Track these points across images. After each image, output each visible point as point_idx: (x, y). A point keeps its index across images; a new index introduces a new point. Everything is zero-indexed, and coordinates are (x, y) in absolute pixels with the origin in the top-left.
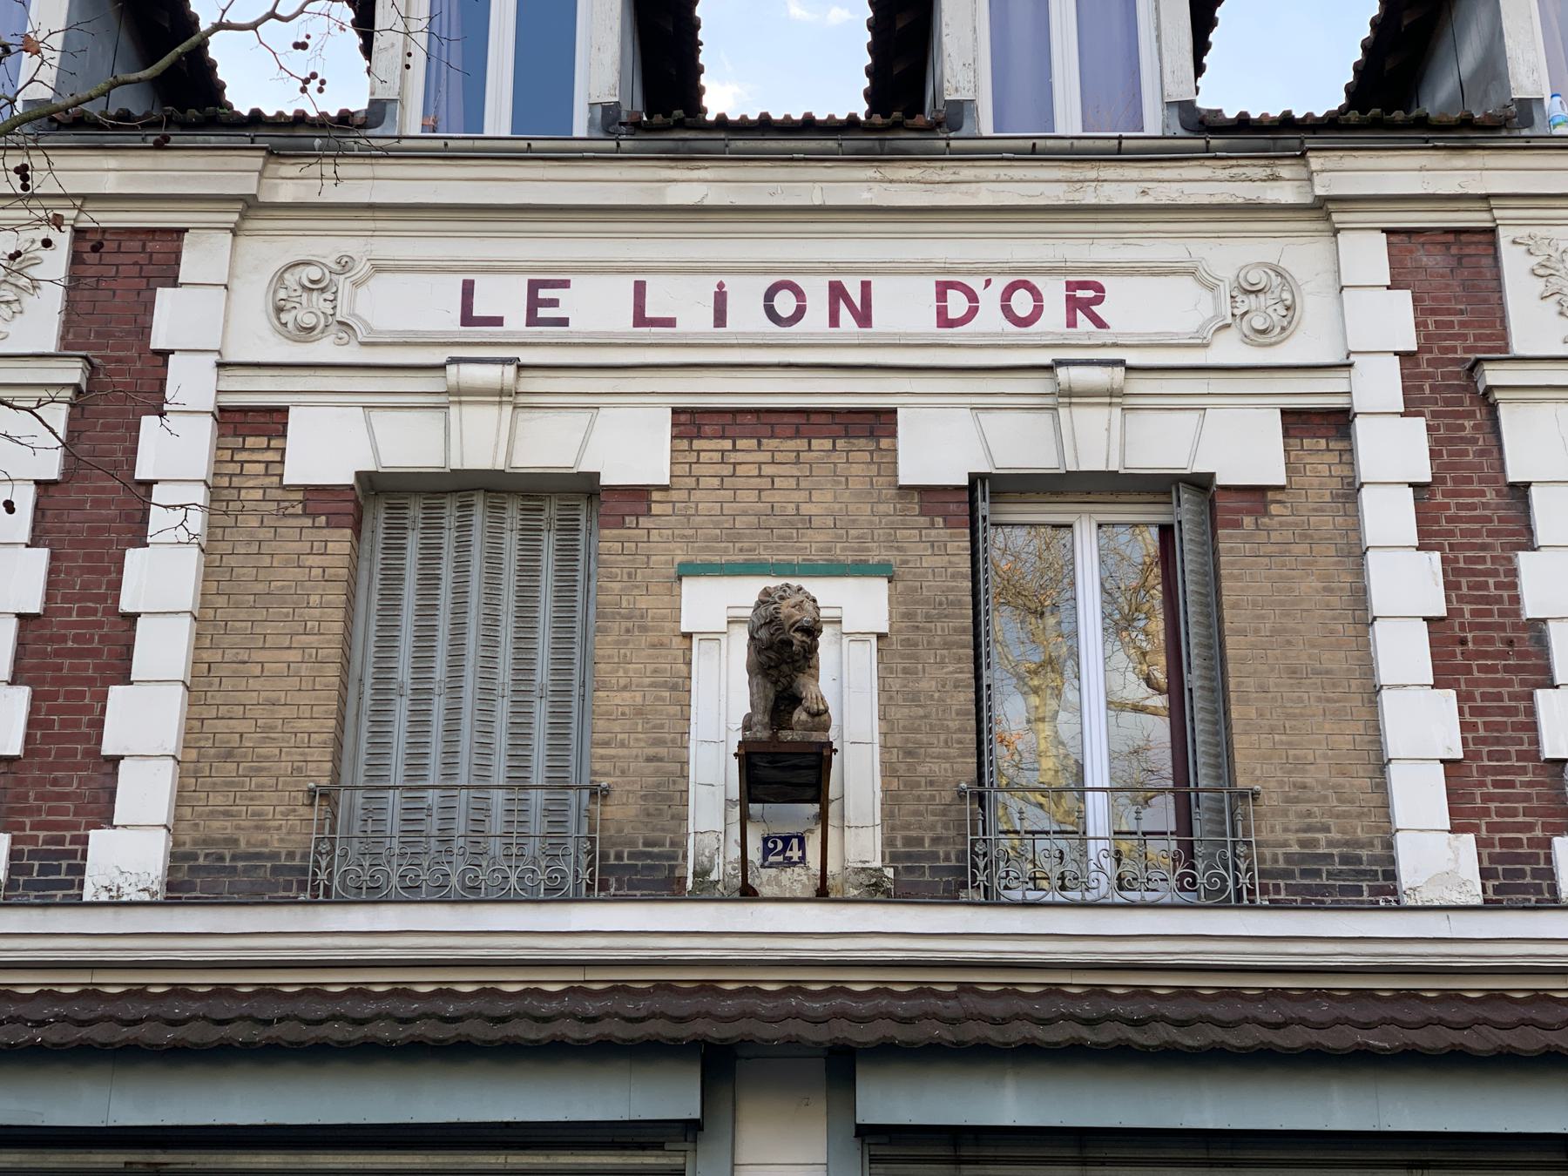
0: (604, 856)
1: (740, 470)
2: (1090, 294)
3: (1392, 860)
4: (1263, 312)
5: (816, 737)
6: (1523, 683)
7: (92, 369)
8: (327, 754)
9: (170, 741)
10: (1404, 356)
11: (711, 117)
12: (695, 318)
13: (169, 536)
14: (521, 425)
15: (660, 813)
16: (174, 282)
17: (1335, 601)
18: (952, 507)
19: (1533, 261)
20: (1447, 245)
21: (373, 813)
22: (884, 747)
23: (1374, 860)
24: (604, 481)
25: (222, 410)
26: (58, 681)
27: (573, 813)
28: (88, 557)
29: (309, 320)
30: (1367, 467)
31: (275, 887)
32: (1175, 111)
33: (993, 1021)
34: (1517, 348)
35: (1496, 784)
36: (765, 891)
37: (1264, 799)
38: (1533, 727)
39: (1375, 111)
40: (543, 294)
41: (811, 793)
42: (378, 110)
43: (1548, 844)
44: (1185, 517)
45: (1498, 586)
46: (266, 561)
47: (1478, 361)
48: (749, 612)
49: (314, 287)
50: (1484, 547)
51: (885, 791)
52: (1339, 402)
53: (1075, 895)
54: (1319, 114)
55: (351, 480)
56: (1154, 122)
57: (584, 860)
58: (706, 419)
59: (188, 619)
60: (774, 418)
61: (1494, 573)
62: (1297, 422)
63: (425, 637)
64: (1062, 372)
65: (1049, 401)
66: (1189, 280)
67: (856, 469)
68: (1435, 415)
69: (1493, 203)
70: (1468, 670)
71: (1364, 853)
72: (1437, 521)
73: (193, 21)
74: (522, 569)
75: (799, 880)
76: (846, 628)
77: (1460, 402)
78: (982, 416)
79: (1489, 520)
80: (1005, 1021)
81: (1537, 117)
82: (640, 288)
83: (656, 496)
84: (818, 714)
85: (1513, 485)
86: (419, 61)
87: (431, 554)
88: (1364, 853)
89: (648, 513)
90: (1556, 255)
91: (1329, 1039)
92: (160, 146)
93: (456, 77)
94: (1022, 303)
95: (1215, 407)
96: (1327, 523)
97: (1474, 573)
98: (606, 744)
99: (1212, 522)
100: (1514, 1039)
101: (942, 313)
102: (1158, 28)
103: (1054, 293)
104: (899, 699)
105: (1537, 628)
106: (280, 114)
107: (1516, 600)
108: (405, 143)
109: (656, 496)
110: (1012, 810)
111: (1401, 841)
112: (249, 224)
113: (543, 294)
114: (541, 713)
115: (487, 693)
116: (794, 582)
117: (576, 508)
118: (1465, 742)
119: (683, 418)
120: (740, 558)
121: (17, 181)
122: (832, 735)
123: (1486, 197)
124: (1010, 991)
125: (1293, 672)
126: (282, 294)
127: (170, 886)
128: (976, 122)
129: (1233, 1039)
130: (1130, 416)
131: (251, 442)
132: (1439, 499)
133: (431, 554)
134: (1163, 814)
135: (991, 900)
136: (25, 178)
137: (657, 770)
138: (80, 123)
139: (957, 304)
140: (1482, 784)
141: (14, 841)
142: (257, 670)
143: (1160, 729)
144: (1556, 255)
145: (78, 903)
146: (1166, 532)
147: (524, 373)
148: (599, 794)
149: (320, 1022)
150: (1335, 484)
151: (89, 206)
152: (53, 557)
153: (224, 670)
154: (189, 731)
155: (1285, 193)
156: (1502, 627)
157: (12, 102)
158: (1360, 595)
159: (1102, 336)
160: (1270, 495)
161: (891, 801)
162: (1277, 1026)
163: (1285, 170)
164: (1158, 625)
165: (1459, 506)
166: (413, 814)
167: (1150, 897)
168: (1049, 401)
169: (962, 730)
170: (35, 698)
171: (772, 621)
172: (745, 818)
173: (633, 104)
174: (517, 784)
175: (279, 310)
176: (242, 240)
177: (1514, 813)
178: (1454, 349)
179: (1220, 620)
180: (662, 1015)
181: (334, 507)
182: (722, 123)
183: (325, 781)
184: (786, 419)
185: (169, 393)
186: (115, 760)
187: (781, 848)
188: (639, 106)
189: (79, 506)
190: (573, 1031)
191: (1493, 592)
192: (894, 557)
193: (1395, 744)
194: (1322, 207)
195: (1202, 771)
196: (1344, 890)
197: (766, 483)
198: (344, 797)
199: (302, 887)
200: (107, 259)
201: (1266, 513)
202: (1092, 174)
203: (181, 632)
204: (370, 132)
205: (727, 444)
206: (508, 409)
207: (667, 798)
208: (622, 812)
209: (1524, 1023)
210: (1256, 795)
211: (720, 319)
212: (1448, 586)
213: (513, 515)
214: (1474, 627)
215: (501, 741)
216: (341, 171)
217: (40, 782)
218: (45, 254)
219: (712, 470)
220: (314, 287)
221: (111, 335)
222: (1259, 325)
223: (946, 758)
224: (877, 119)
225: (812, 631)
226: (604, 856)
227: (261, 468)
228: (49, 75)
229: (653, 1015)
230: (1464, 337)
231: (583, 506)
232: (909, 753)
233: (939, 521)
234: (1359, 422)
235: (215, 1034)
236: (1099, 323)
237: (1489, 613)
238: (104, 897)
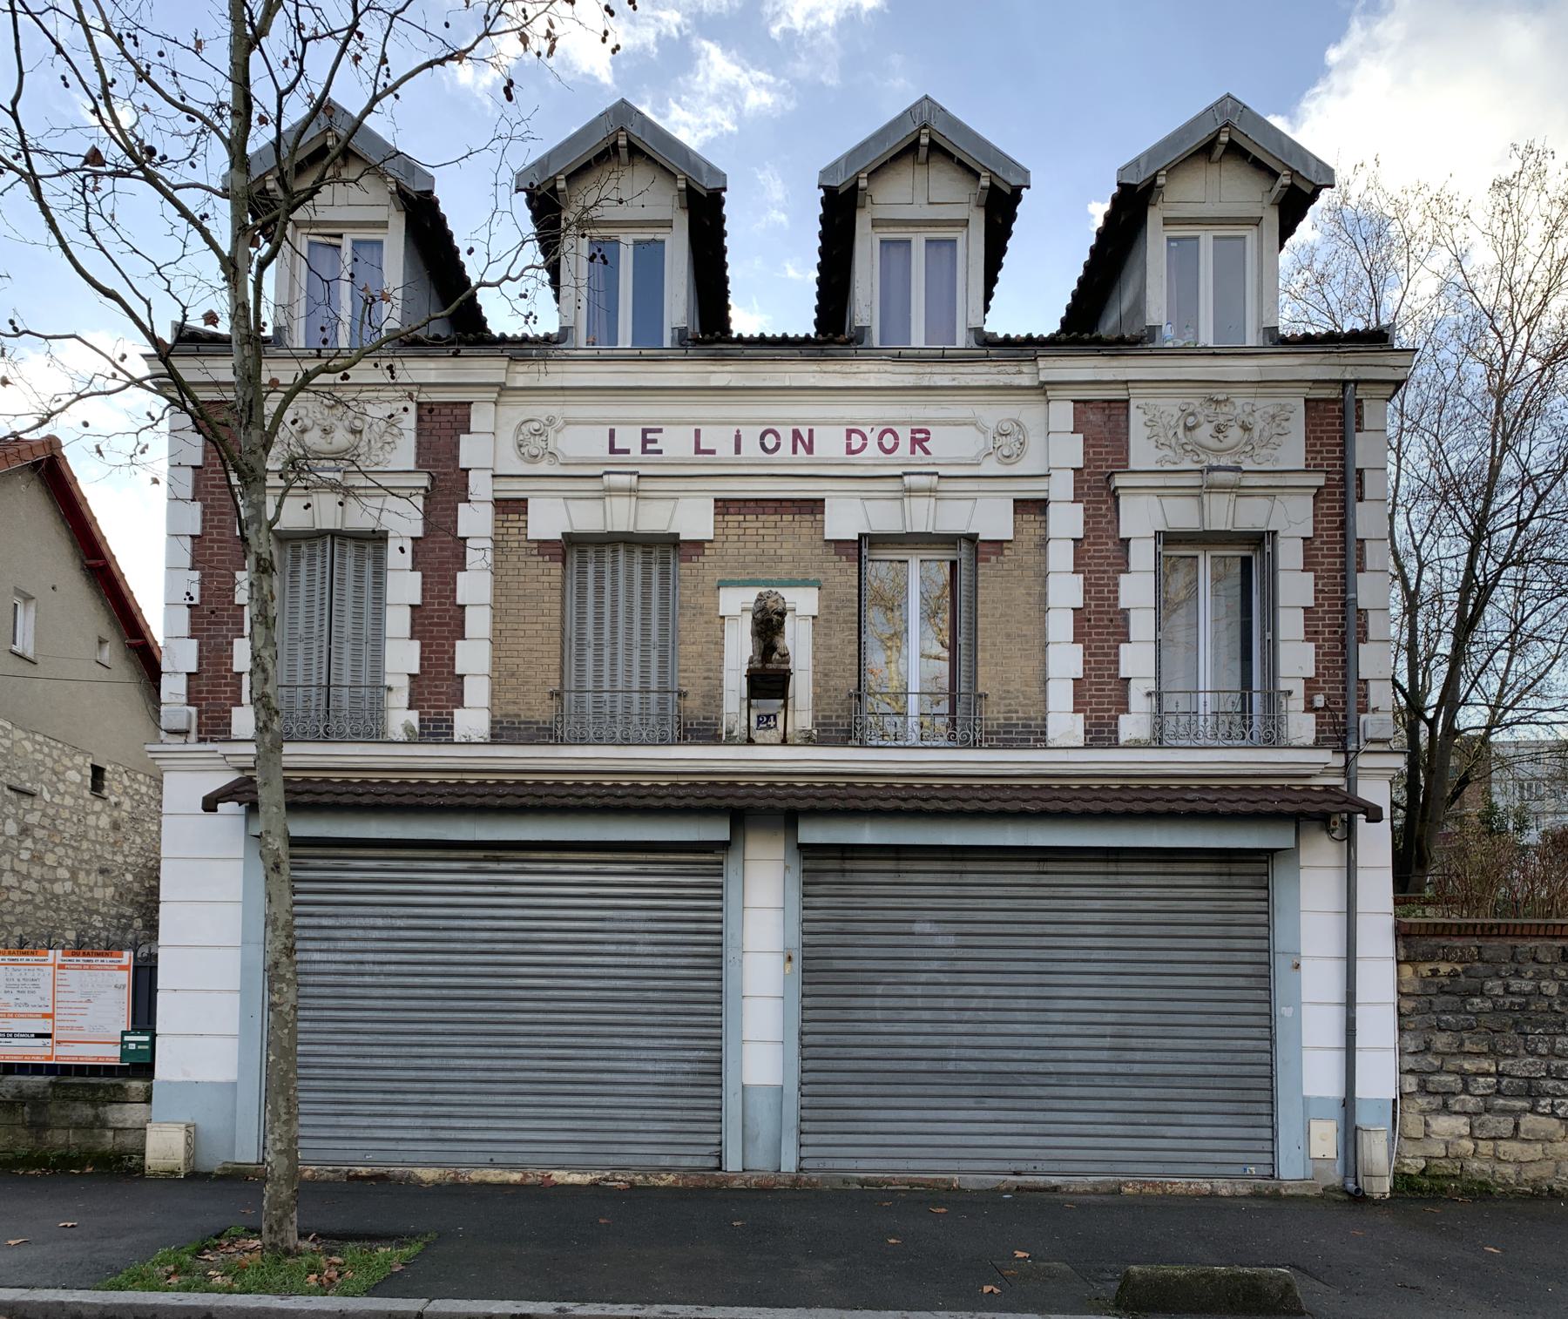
0: (685, 724)
1: (748, 531)
2: (923, 436)
3: (1045, 726)
4: (1008, 448)
5: (783, 666)
6: (1115, 640)
7: (433, 479)
8: (557, 675)
9: (486, 669)
10: (1076, 470)
11: (734, 335)
12: (725, 451)
13: (477, 565)
14: (640, 508)
15: (710, 704)
16: (468, 432)
17: (1031, 600)
18: (851, 551)
19: (1147, 417)
20: (1104, 409)
21: (580, 703)
22: (814, 672)
23: (1037, 726)
24: (682, 538)
25: (496, 500)
26: (432, 638)
27: (670, 704)
28: (440, 576)
29: (535, 452)
30: (1053, 531)
31: (538, 736)
32: (973, 333)
33: (862, 799)
34: (1132, 467)
35: (1096, 690)
36: (758, 741)
37: (990, 698)
38: (1117, 662)
39: (1074, 334)
40: (650, 436)
41: (780, 694)
42: (565, 332)
43: (1117, 718)
44: (963, 557)
45: (1109, 592)
46: (522, 579)
47: (1113, 473)
48: (752, 606)
49: (537, 433)
50: (1104, 572)
51: (814, 694)
52: (1041, 495)
53: (901, 743)
54: (1046, 335)
55: (560, 537)
56: (962, 340)
57: (676, 726)
58: (731, 504)
59: (488, 608)
60: (764, 504)
61: (1108, 585)
62: (1021, 506)
63: (599, 618)
64: (906, 479)
65: (899, 494)
66: (972, 428)
67: (804, 531)
68: (1088, 502)
69: (1130, 385)
70: (1090, 634)
71: (1033, 723)
72: (1083, 558)
73: (468, 281)
74: (643, 583)
75: (773, 735)
76: (797, 613)
77: (1101, 495)
78: (866, 503)
79: (1109, 557)
80: (866, 799)
81: (1158, 336)
82: (698, 432)
83: (707, 545)
84: (785, 655)
85: (1122, 540)
86: (584, 304)
87: (600, 576)
88: (1033, 723)
89: (703, 555)
90: (1158, 414)
91: (1009, 806)
92: (455, 355)
93: (603, 313)
94: (888, 441)
95: (981, 498)
96: (1030, 560)
97: (1098, 585)
98: (685, 671)
99: (976, 559)
100: (1090, 806)
101: (849, 446)
102: (967, 285)
103: (905, 435)
104: (822, 649)
105: (1125, 613)
106: (515, 336)
107: (1117, 599)
108: (579, 352)
109: (707, 545)
110: (871, 703)
111: (1050, 717)
112: (503, 399)
113: (650, 436)
114: (654, 655)
115: (629, 647)
116: (774, 590)
117: (668, 552)
118: (1084, 670)
119: (720, 504)
120: (747, 578)
121: (388, 373)
122: (791, 666)
123: (1126, 382)
124: (869, 786)
125: (1008, 636)
126: (521, 437)
127: (492, 736)
128: (871, 339)
129: (967, 806)
130: (939, 502)
131: (511, 517)
132: (1086, 547)
133: (600, 576)
134: (944, 707)
135: (862, 745)
136: (392, 372)
137: (709, 684)
138: (415, 342)
139: (856, 442)
140: (1090, 690)
141: (421, 714)
142: (522, 634)
143: (944, 667)
144: (1158, 414)
145: (453, 743)
146: (953, 564)
147: (642, 480)
148: (682, 695)
149: (563, 797)
150: (1036, 539)
151: (424, 389)
152: (424, 576)
153: (506, 633)
154: (494, 663)
155: (1025, 380)
156: (1108, 613)
157: (380, 330)
158: (1043, 597)
159: (928, 459)
160: (1005, 545)
161: (817, 698)
162: (986, 801)
163: (1026, 368)
164: (947, 616)
165: (1095, 551)
166: (598, 704)
167: (935, 744)
168: (899, 494)
169: (851, 664)
170: (423, 646)
171: (763, 609)
172: (749, 706)
173: (694, 329)
174: (645, 690)
175: (520, 446)
176: (500, 408)
177: (1103, 704)
178: (1101, 467)
179: (976, 609)
180: (712, 796)
181: (551, 551)
182: (740, 339)
183: (557, 688)
184: (770, 504)
185: (471, 489)
186: (462, 677)
187: (766, 720)
188: (697, 330)
189: (433, 550)
190: (674, 803)
191: (1106, 595)
192: (821, 577)
193: (1052, 672)
194: (1042, 388)
195: (962, 684)
196: (1022, 740)
197: (760, 538)
198: (566, 695)
199: (551, 737)
200: (435, 419)
201: (1002, 554)
202: (929, 370)
203: (487, 613)
204: (561, 346)
205: (741, 518)
206: (634, 499)
207: (714, 697)
208: (693, 704)
209: (1095, 799)
210: (986, 696)
211: (738, 451)
212: (1086, 592)
213: (638, 556)
214: (1095, 612)
215: (637, 670)
216: (550, 368)
217: (429, 686)
218: (404, 416)
219: (733, 531)
220: (537, 433)
221: (440, 461)
222: (1007, 454)
223: (844, 677)
224: (820, 337)
225: (782, 614)
226: (685, 724)
227: (516, 531)
228: (397, 314)
229: (708, 796)
230: (1107, 460)
231: (672, 550)
232: (826, 675)
233: (844, 558)
234: (1051, 506)
235: (518, 801)
236: (927, 452)
237: (1103, 606)
238: (463, 740)
